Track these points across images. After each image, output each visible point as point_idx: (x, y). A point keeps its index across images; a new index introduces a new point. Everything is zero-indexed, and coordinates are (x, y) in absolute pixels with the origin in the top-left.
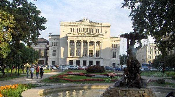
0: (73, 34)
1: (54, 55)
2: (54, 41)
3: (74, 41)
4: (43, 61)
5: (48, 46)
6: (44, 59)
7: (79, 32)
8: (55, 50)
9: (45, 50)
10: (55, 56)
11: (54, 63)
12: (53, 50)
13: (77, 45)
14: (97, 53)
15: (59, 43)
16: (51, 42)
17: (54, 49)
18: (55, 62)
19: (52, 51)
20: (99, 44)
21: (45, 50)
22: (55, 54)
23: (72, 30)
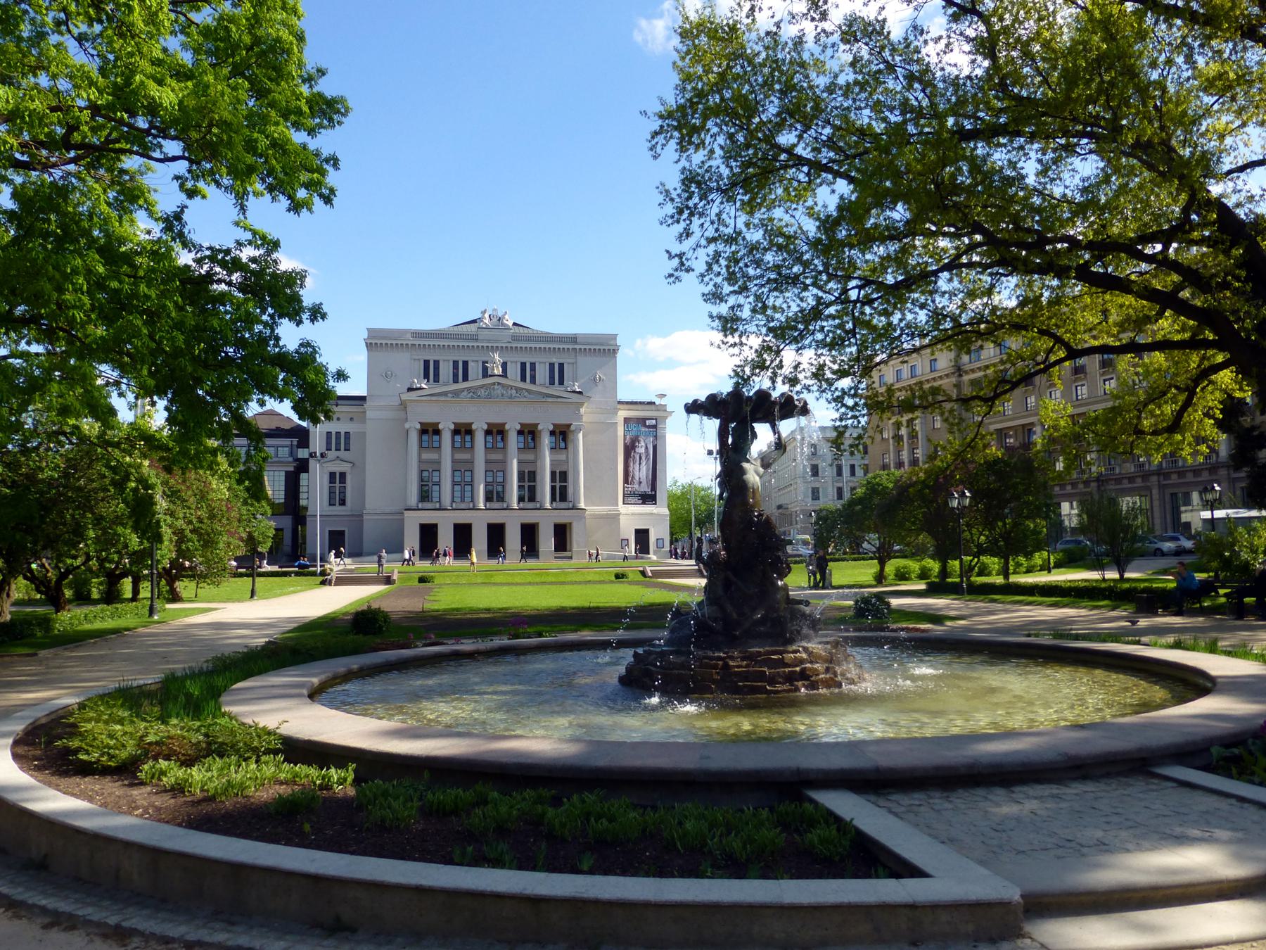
1: (337, 495)
3: (440, 427)
5: (303, 453)
7: (466, 378)
8: (343, 475)
12: (332, 475)
13: (490, 445)
14: (558, 485)
15: (363, 435)
19: (326, 478)
20: (565, 440)
21: (287, 473)
22: (343, 492)
23: (430, 371)
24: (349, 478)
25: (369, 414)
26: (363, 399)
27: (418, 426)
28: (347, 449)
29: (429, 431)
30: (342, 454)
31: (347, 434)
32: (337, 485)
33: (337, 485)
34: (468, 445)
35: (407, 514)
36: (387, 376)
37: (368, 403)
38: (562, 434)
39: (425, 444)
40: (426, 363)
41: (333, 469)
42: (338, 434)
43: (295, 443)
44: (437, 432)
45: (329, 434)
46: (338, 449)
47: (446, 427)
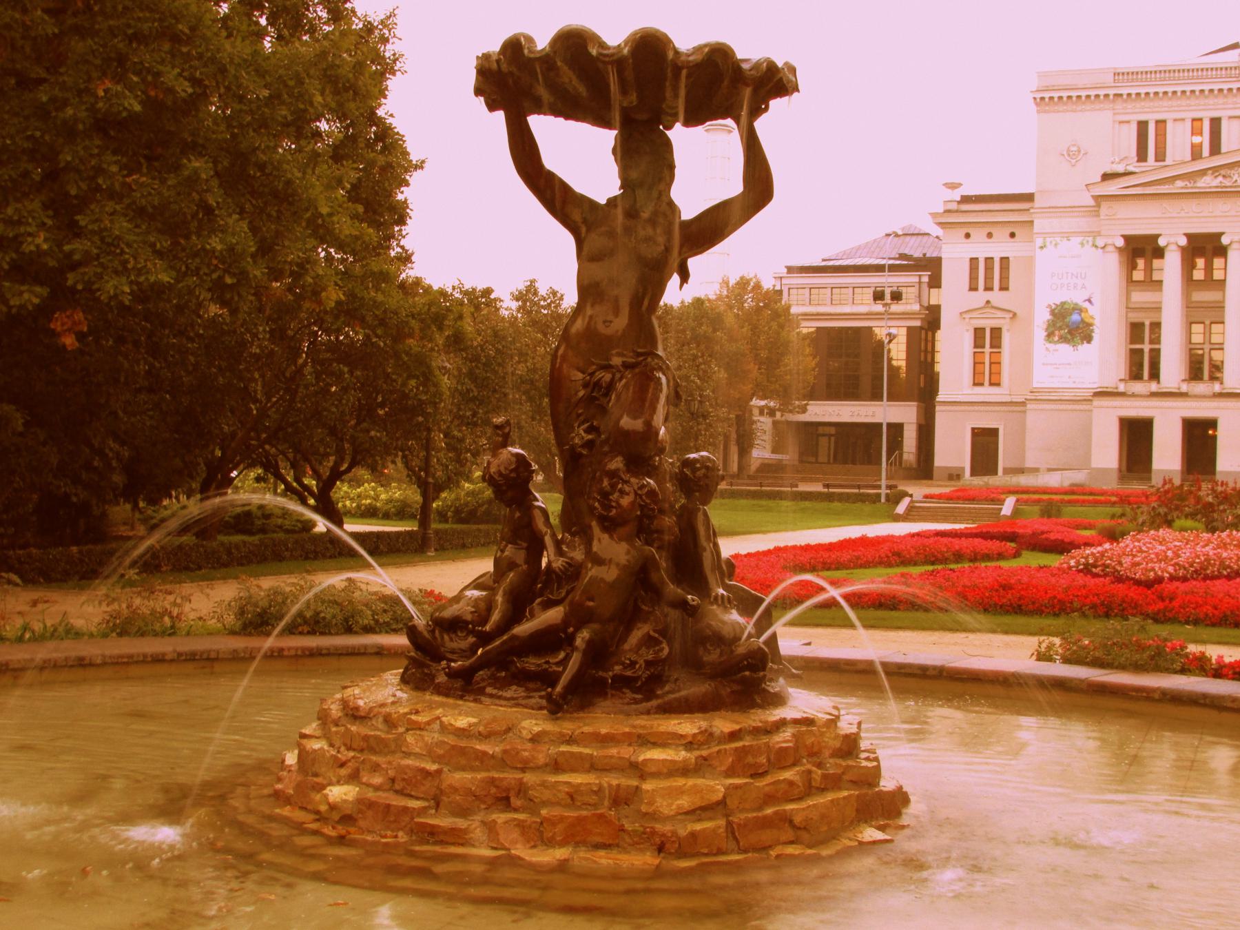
0: (1151, 169)
1: (986, 370)
2: (982, 248)
3: (1162, 242)
4: (896, 430)
5: (935, 297)
6: (905, 414)
7: (1215, 149)
8: (996, 333)
9: (909, 328)
10: (995, 383)
11: (985, 445)
12: (979, 333)
14: (1146, 347)
15: (1030, 262)
16: (956, 255)
17: (988, 324)
18: (994, 432)
19: (969, 339)
21: (910, 330)
22: (996, 363)
23: (1147, 140)
24: (1006, 338)
25: (1038, 225)
26: (1029, 198)
27: (1183, 241)
28: (1004, 288)
29: (1141, 250)
30: (996, 297)
31: (1005, 261)
32: (987, 349)
33: (987, 349)
34: (1218, 275)
35: (1097, 402)
36: (1074, 154)
37: (1038, 202)
38: (1204, 248)
39: (1198, 275)
40: (1142, 126)
41: (980, 323)
42: (989, 260)
43: (925, 279)
44: (1159, 253)
45: (974, 261)
46: (988, 288)
47: (1173, 239)
